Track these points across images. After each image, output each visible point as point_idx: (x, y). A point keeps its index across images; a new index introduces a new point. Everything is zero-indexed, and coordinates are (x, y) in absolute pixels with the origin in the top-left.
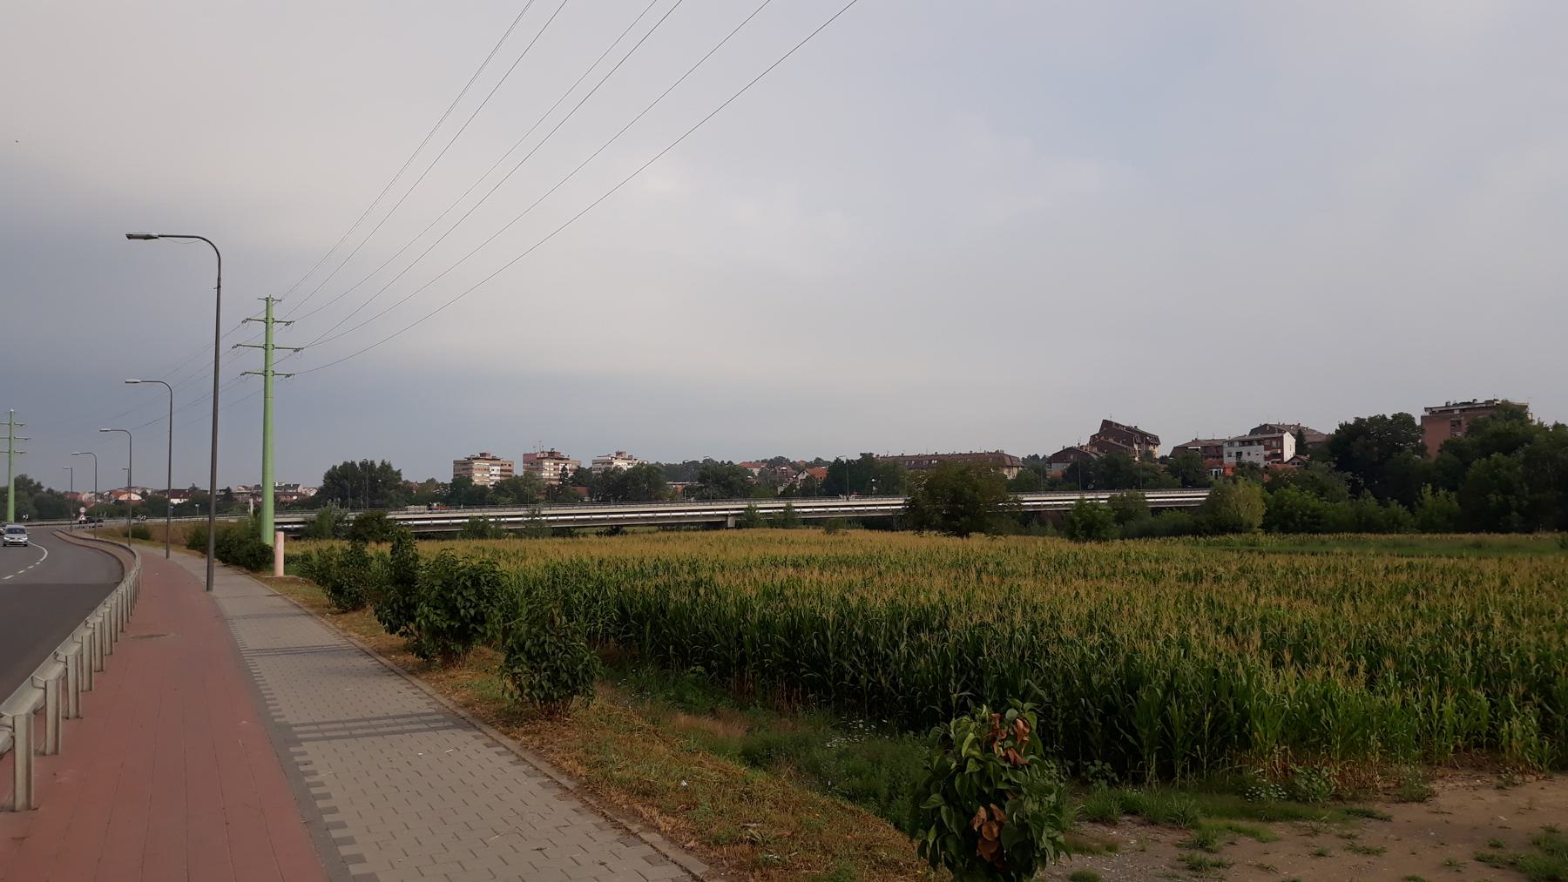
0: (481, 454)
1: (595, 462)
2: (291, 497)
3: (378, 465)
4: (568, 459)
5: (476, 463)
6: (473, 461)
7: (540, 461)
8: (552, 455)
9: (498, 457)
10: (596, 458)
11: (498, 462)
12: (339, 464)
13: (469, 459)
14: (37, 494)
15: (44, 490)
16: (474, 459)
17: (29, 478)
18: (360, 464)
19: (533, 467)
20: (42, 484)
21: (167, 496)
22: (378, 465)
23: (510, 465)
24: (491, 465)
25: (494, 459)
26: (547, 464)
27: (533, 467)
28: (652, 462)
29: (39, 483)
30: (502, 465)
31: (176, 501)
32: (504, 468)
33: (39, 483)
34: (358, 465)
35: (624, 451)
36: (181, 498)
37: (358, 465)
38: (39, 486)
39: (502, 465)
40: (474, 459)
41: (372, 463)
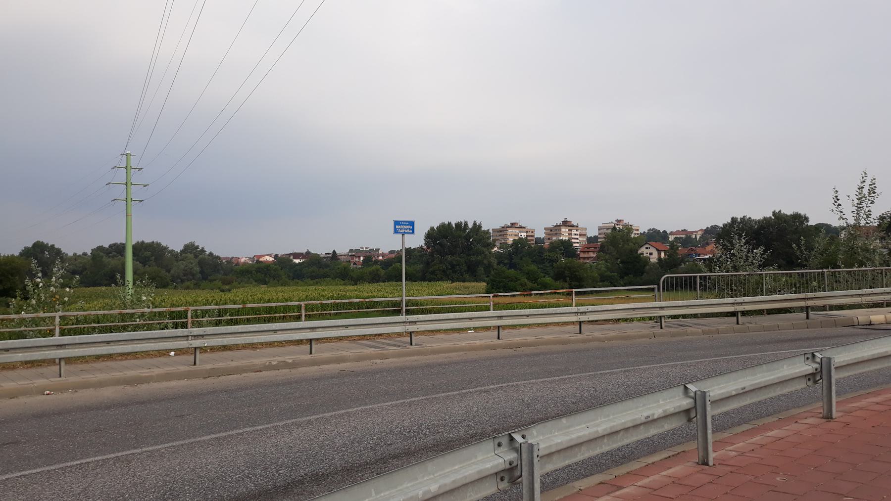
0: (512, 224)
1: (600, 228)
2: (378, 257)
3: (470, 225)
4: (577, 226)
5: (510, 231)
6: (508, 229)
7: (558, 228)
8: (566, 223)
9: (523, 225)
10: (601, 225)
11: (523, 230)
12: (436, 225)
13: (503, 227)
14: (200, 256)
15: (207, 253)
16: (510, 227)
17: (196, 244)
18: (456, 224)
19: (551, 233)
20: (205, 249)
21: (292, 257)
22: (470, 225)
23: (532, 232)
24: (520, 232)
25: (521, 227)
26: (563, 230)
27: (551, 233)
28: (658, 229)
29: (203, 248)
30: (527, 232)
31: (297, 261)
32: (529, 234)
33: (203, 248)
34: (454, 226)
35: (622, 219)
36: (300, 259)
37: (454, 226)
38: (203, 251)
39: (527, 232)
40: (507, 227)
41: (466, 224)
